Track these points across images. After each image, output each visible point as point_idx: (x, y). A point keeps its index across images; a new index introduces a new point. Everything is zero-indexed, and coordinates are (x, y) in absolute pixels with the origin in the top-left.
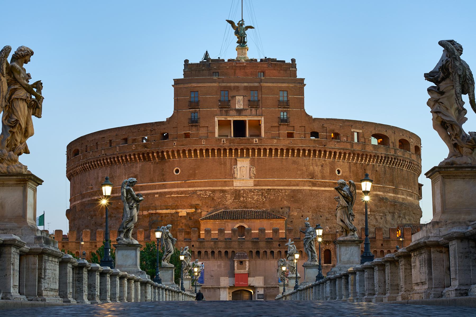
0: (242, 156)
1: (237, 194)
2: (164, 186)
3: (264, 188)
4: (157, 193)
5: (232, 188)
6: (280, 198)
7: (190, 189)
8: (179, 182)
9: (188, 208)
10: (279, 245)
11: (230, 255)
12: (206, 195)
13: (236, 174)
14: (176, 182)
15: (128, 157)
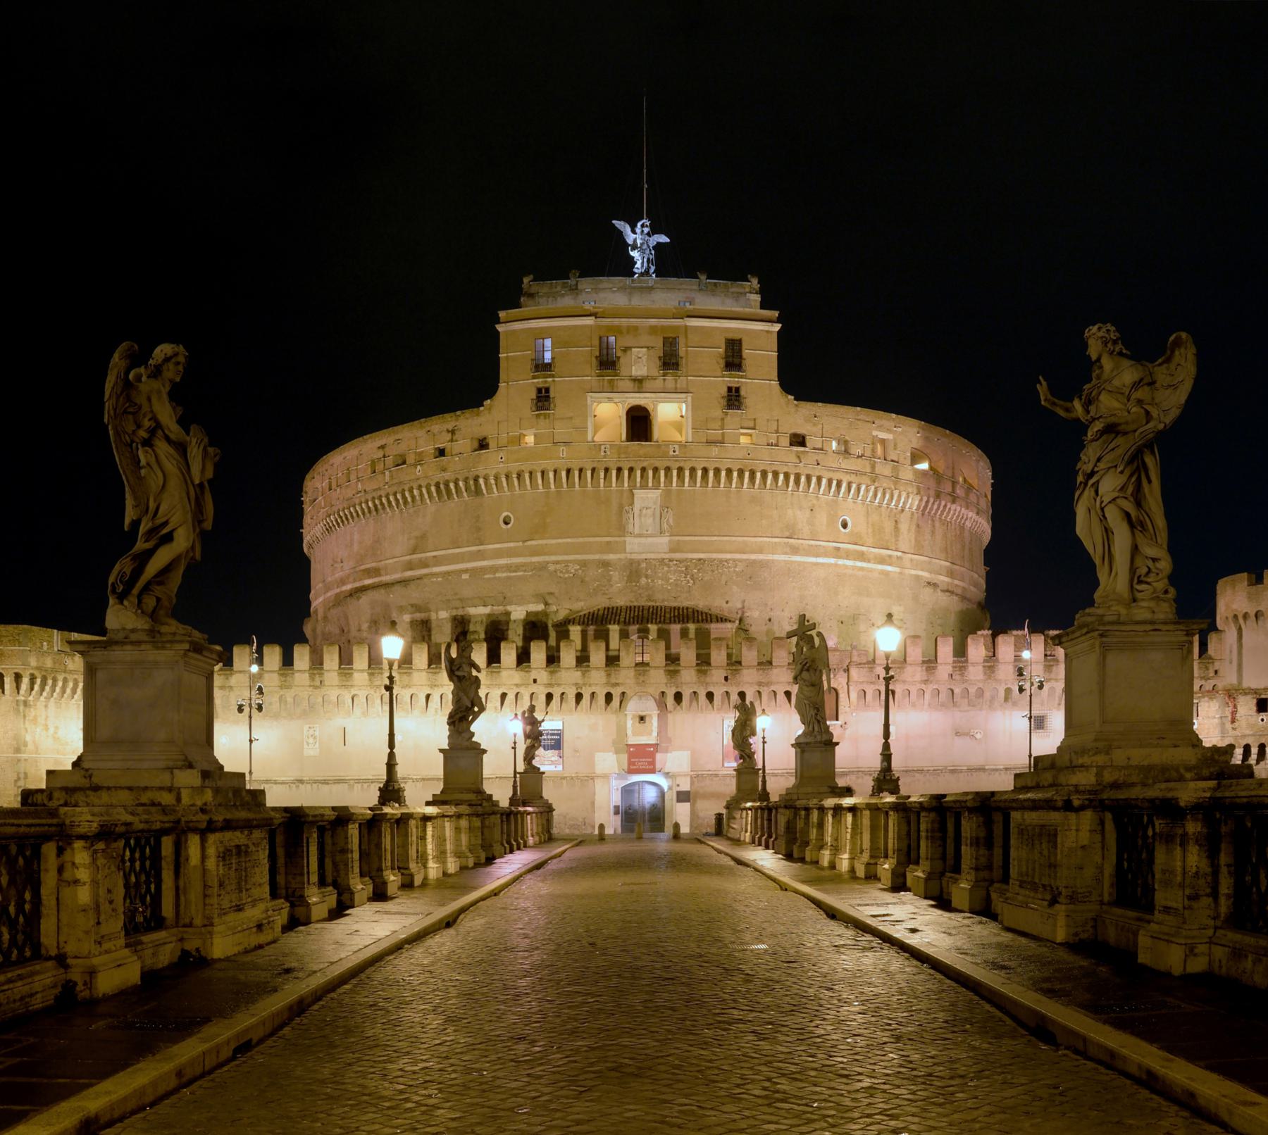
0: (644, 486)
1: (634, 571)
2: (480, 555)
3: (690, 556)
4: (466, 571)
5: (622, 556)
6: (724, 578)
7: (535, 559)
8: (512, 545)
9: (529, 603)
10: (726, 679)
11: (616, 701)
12: (568, 572)
13: (631, 526)
14: (506, 545)
15: (407, 494)
